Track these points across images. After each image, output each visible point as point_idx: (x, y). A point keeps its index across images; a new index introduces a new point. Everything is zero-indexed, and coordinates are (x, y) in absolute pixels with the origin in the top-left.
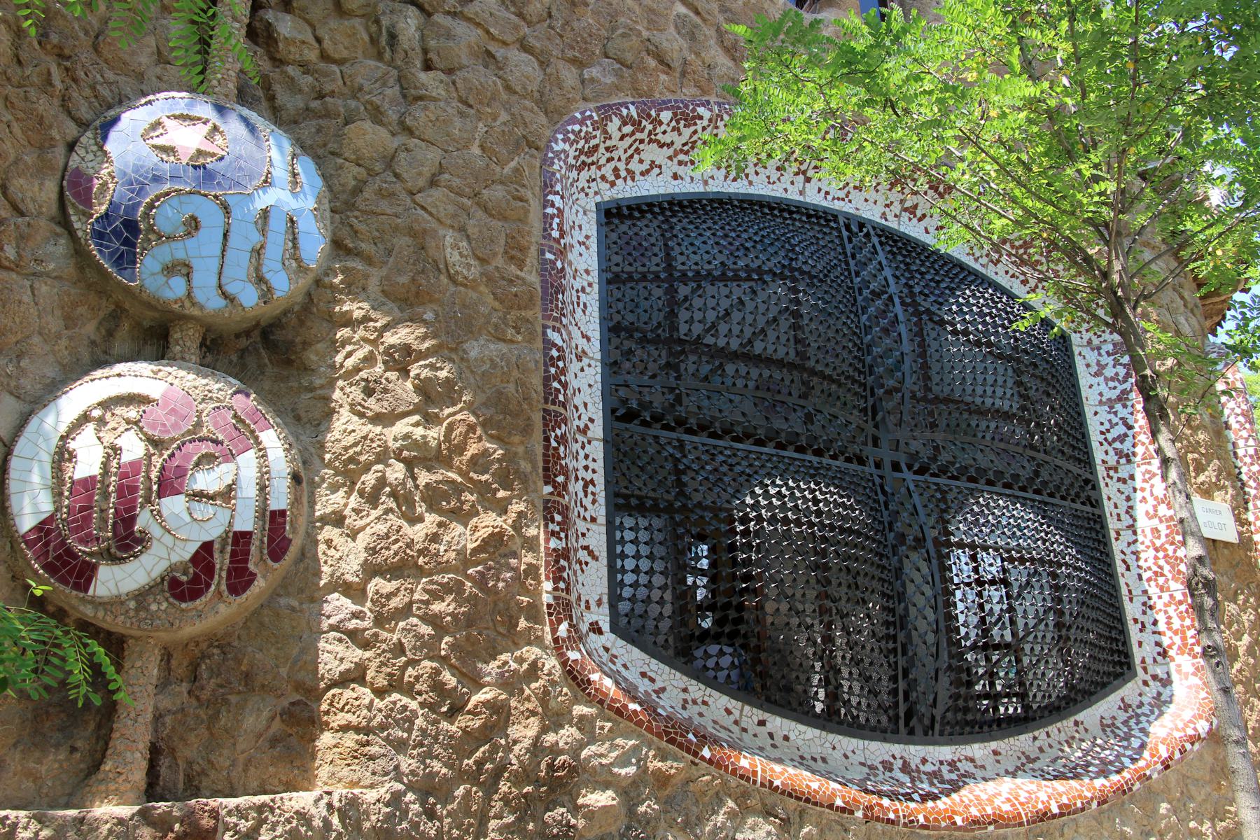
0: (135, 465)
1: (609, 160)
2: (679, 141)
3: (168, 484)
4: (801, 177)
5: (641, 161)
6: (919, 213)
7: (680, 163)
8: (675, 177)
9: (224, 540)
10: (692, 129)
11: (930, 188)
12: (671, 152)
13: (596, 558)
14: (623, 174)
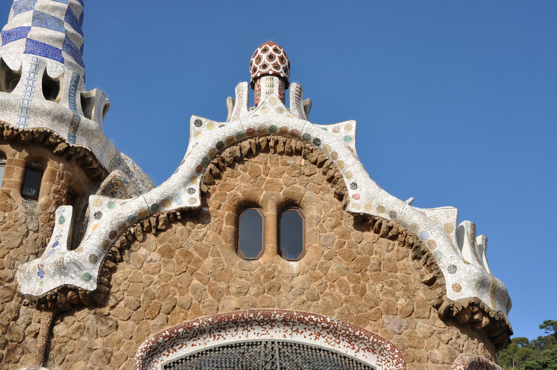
7: (194, 341)
12: (188, 338)
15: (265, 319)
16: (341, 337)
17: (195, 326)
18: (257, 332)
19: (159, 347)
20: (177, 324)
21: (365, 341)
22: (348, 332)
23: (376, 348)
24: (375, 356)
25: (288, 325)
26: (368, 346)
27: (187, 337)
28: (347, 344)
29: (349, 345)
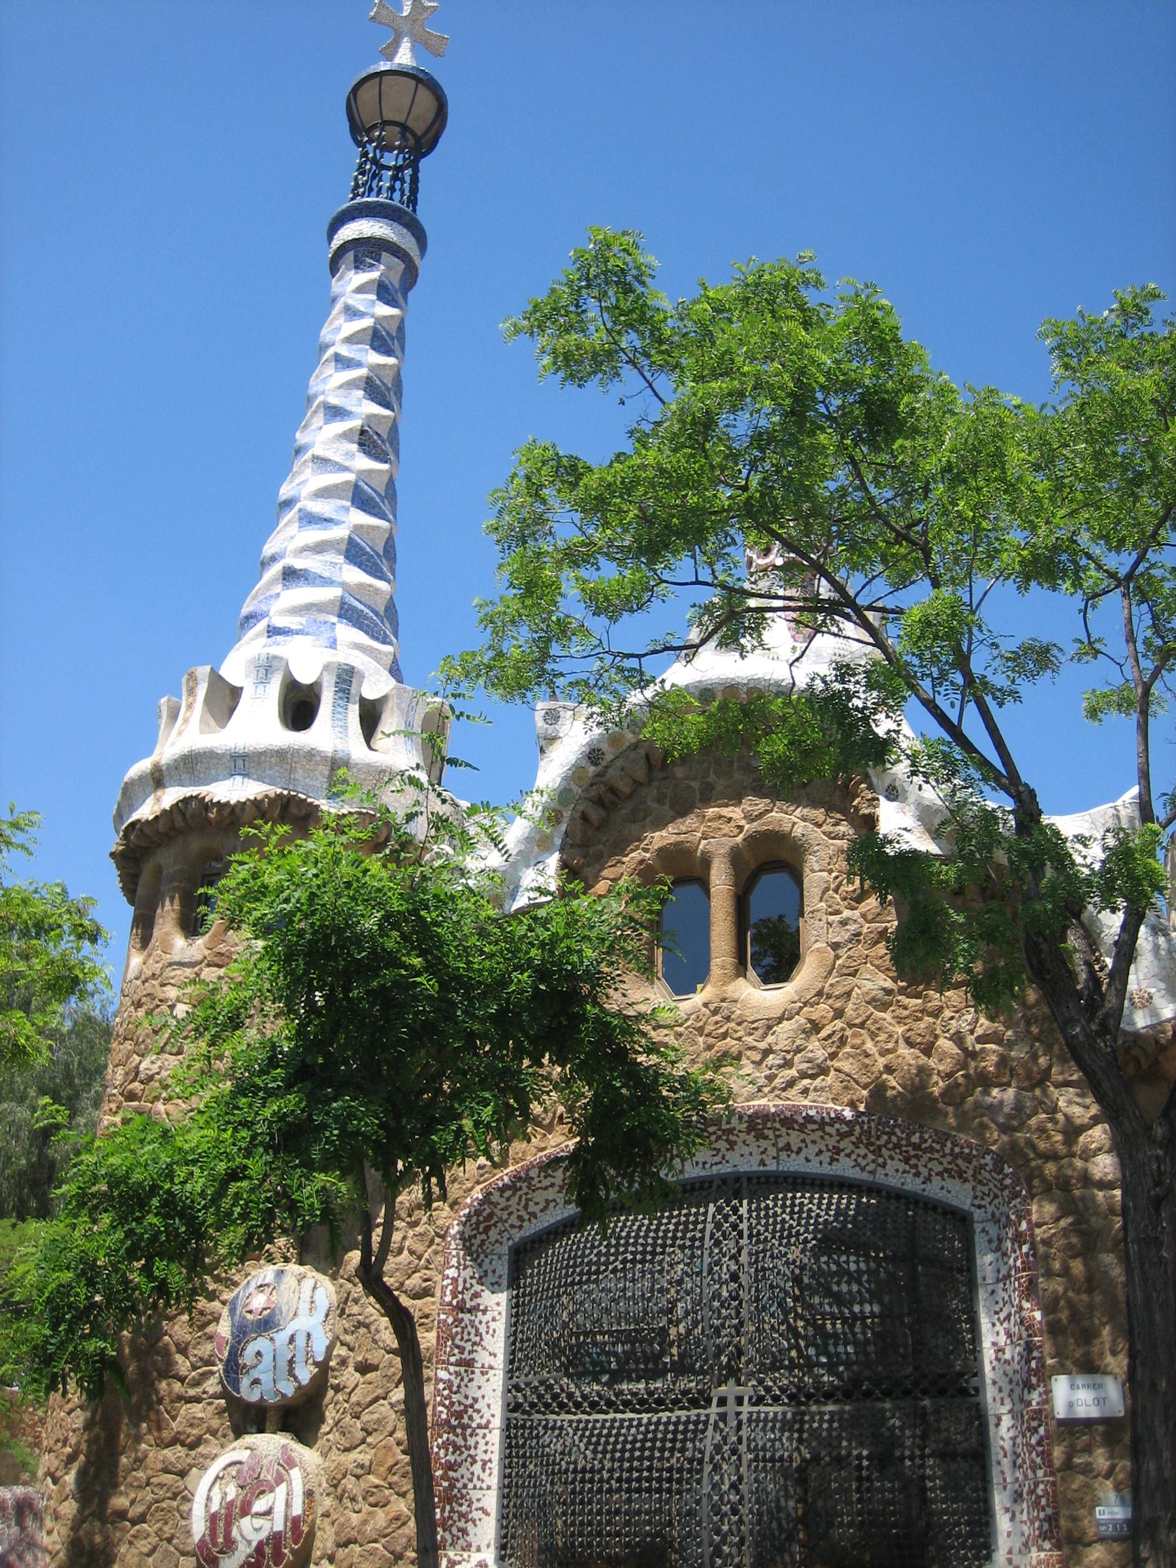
0: (232, 1502)
1: (510, 1214)
3: (245, 1511)
6: (795, 1148)
9: (268, 1539)
12: (556, 1188)
13: (488, 1514)
14: (526, 1217)
18: (701, 1160)
20: (530, 1158)
21: (936, 1155)
22: (894, 1139)
24: (968, 1186)
25: (766, 1138)
26: (946, 1165)
27: (552, 1185)
28: (902, 1166)
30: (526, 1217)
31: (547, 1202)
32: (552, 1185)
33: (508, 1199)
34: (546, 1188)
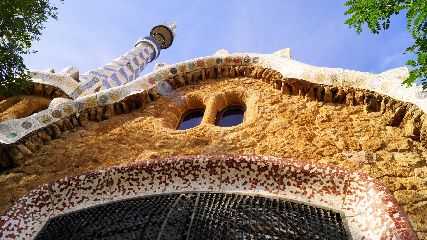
1: (59, 201)
2: (94, 186)
4: (163, 184)
5: (77, 198)
7: (98, 194)
8: (96, 200)
10: (98, 179)
11: (229, 167)
12: (92, 191)
14: (68, 204)
15: (187, 166)
16: (285, 180)
17: (101, 174)
19: (53, 197)
23: (337, 184)
25: (216, 173)
27: (90, 188)
28: (295, 189)
29: (298, 190)
30: (68, 204)
31: (83, 198)
32: (90, 188)
33: (62, 190)
34: (86, 189)
